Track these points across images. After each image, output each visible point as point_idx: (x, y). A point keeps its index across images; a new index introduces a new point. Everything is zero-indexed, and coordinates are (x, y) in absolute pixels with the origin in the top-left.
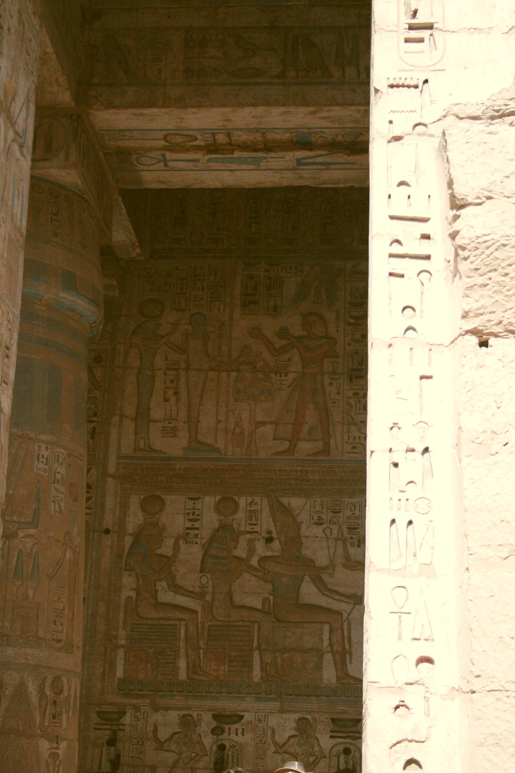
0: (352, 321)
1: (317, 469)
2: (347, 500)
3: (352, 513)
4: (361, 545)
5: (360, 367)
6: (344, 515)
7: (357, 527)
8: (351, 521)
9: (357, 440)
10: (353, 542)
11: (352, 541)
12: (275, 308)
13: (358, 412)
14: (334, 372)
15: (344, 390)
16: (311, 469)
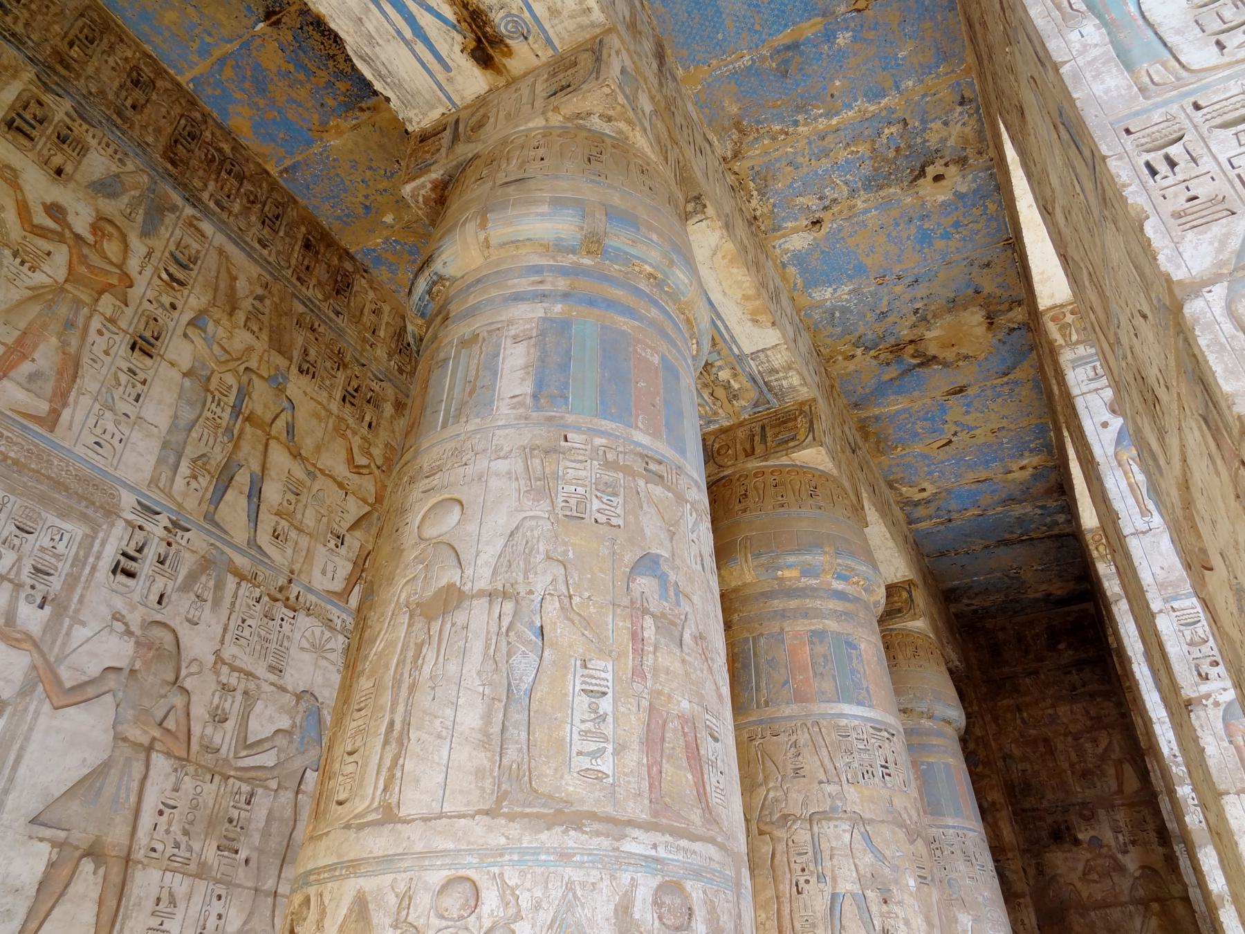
0: (165, 276)
1: (20, 440)
2: (52, 519)
3: (52, 544)
4: (46, 607)
5: (153, 341)
6: (37, 540)
7: (52, 572)
8: (47, 557)
9: (107, 436)
10: (33, 596)
11: (33, 592)
12: (59, 172)
13: (126, 397)
14: (112, 321)
15: (116, 354)
16: (10, 435)
